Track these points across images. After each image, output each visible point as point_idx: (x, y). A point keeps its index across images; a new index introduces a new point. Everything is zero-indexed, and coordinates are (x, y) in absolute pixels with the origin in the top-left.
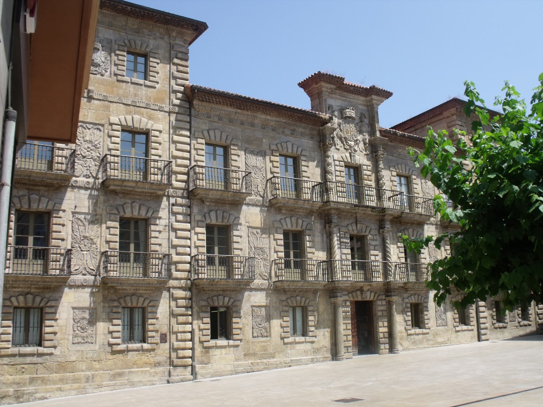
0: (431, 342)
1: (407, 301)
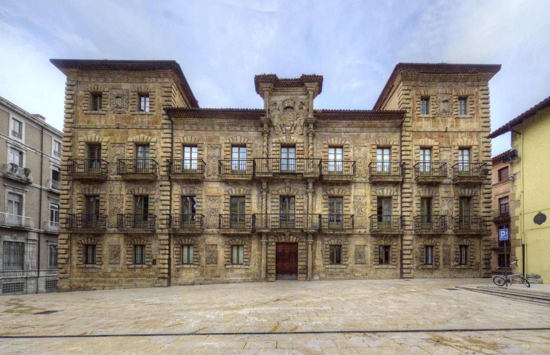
1: (327, 243)
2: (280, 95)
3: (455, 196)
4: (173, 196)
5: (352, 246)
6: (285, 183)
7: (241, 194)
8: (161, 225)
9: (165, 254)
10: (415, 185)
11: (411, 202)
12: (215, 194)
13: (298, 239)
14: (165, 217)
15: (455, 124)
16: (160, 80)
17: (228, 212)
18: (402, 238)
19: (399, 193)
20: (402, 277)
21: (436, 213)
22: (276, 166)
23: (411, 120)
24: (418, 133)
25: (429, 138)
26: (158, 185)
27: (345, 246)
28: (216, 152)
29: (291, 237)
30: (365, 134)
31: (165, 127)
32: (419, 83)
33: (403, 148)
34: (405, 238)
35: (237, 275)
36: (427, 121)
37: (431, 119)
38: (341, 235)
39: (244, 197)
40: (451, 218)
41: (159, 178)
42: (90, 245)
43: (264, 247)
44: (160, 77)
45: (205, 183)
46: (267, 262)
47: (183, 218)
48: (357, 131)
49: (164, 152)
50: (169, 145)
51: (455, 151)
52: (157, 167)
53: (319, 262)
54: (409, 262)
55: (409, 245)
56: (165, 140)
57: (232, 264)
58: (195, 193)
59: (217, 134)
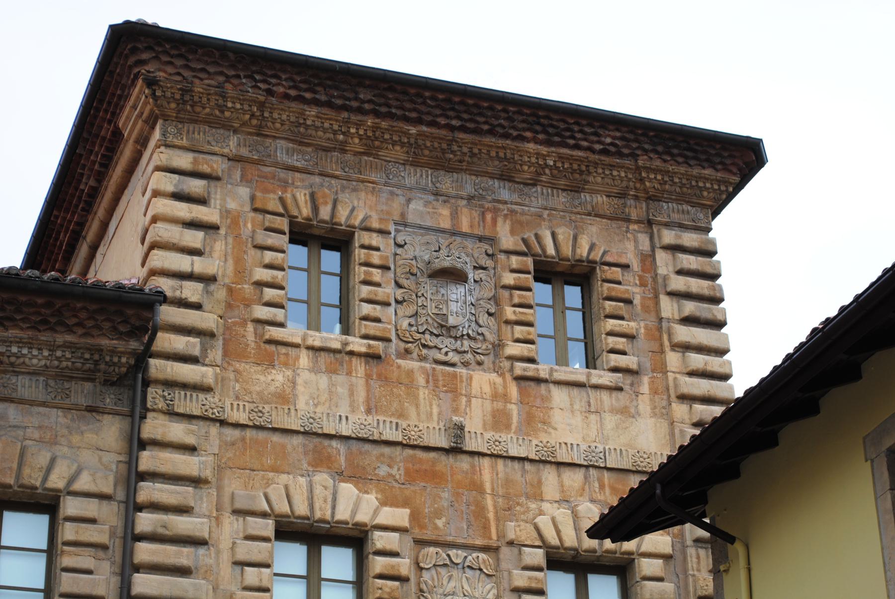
23: (216, 354)
25: (341, 475)
32: (281, 151)
33: (145, 521)
36: (331, 371)
37: (360, 367)
51: (521, 579)
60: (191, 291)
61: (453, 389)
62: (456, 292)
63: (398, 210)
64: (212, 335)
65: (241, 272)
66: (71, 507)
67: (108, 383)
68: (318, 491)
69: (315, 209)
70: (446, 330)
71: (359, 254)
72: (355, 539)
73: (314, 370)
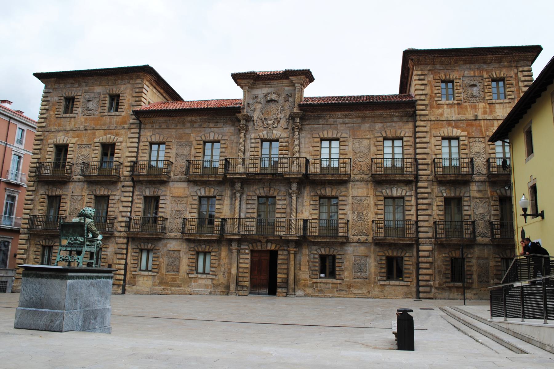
0: (344, 292)
1: (316, 252)
2: (262, 88)
3: (492, 196)
4: (135, 197)
5: (350, 255)
6: (264, 183)
7: (211, 194)
8: (120, 227)
9: (122, 259)
10: (435, 183)
11: (429, 204)
12: (181, 195)
13: (278, 246)
14: (125, 219)
15: (488, 110)
16: (131, 81)
17: (196, 215)
18: (418, 248)
19: (413, 193)
20: (418, 298)
21: (466, 217)
22: (253, 164)
23: (428, 108)
24: (438, 123)
25: (454, 127)
26: (120, 185)
27: (340, 257)
28: (186, 151)
29: (269, 245)
30: (367, 125)
31: (133, 126)
32: (438, 67)
34: (421, 247)
35: (200, 286)
36: (451, 108)
37: (456, 106)
38: (334, 243)
39: (214, 197)
40: (487, 223)
41: (122, 179)
42: (47, 246)
43: (235, 255)
44: (132, 79)
45: (171, 184)
46: (238, 272)
47: (145, 221)
48: (357, 122)
49: (130, 152)
50: (136, 145)
52: (121, 167)
53: (304, 275)
54: (427, 278)
55: (428, 257)
56: (131, 140)
57: (197, 273)
58: (159, 193)
59: (188, 131)
60: (423, 97)
61: (475, 108)
62: (475, 89)
63: (462, 74)
64: (427, 105)
65: (432, 92)
66: (405, 139)
67: (409, 116)
68: (449, 131)
69: (446, 77)
70: (473, 96)
71: (455, 84)
72: (457, 138)
73: (447, 108)
